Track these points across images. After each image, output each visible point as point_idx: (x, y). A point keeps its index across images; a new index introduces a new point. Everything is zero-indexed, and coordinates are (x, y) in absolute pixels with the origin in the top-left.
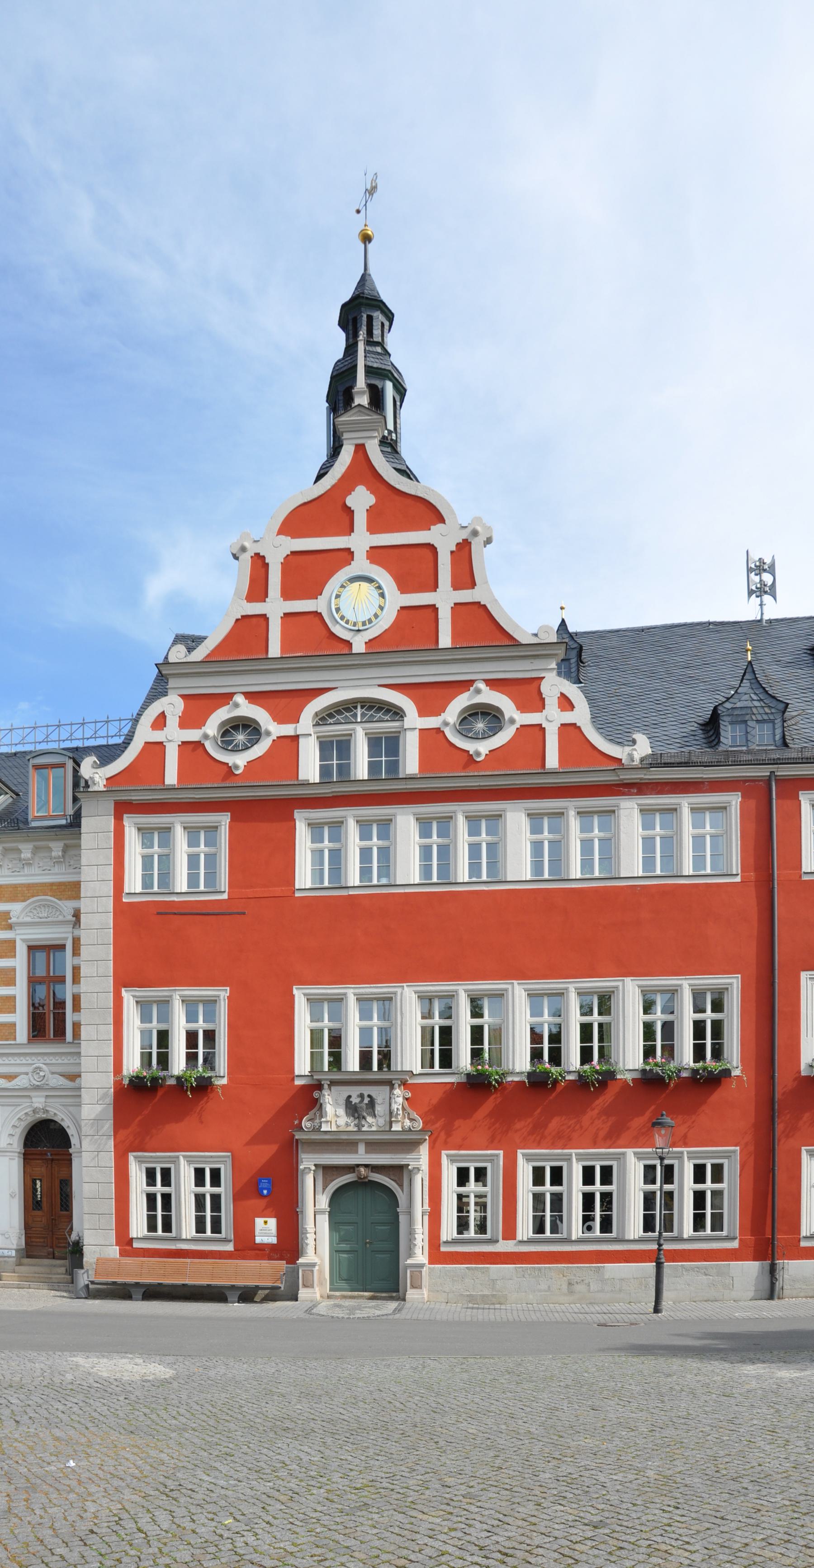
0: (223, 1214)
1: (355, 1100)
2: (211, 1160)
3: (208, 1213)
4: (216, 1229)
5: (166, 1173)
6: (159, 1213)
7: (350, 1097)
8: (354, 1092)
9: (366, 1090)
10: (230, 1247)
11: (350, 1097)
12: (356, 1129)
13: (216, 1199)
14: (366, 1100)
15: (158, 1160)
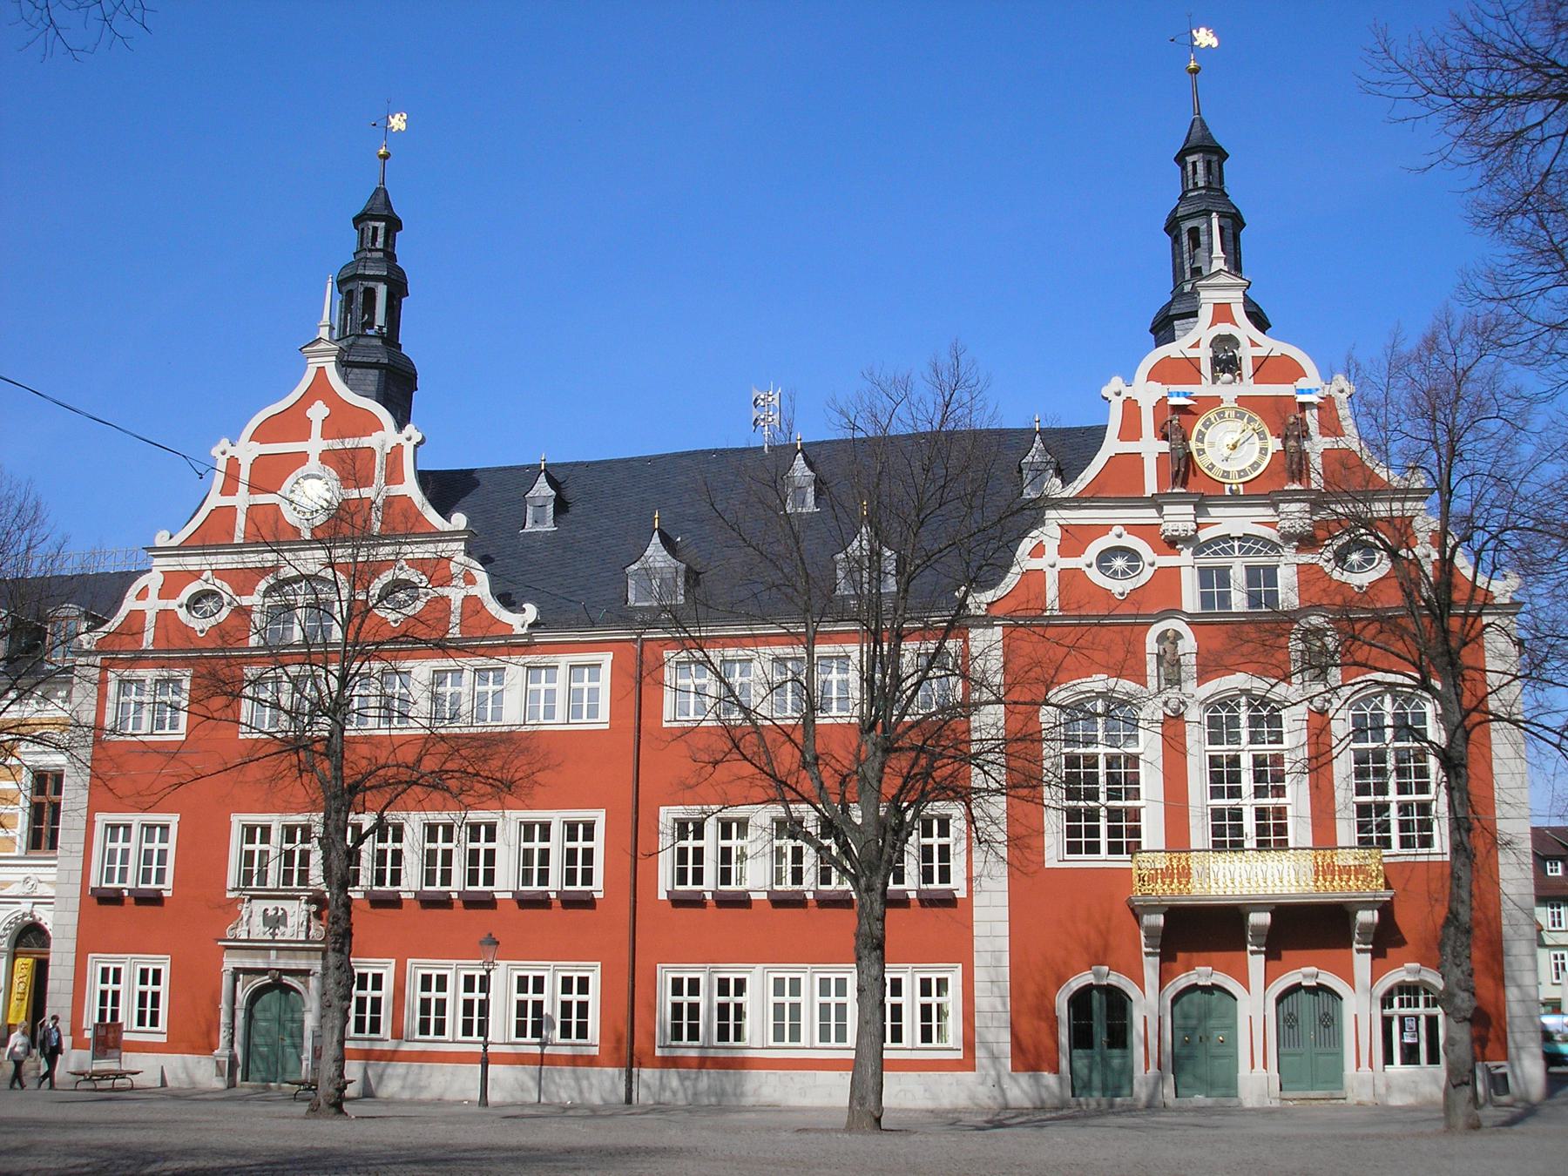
0: (161, 1010)
1: (271, 913)
2: (151, 962)
3: (149, 1009)
4: (154, 1023)
5: (117, 972)
6: (109, 1007)
7: (266, 910)
8: (270, 905)
9: (280, 904)
10: (163, 1039)
11: (266, 910)
12: (270, 938)
13: (156, 996)
14: (280, 913)
15: (111, 961)
